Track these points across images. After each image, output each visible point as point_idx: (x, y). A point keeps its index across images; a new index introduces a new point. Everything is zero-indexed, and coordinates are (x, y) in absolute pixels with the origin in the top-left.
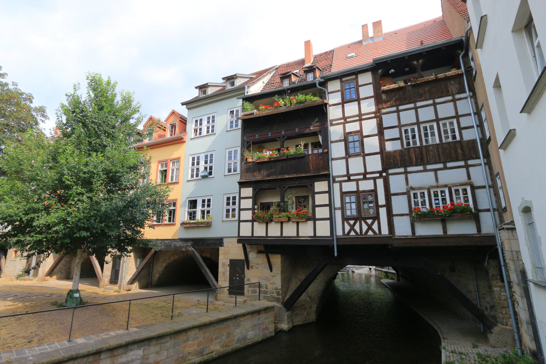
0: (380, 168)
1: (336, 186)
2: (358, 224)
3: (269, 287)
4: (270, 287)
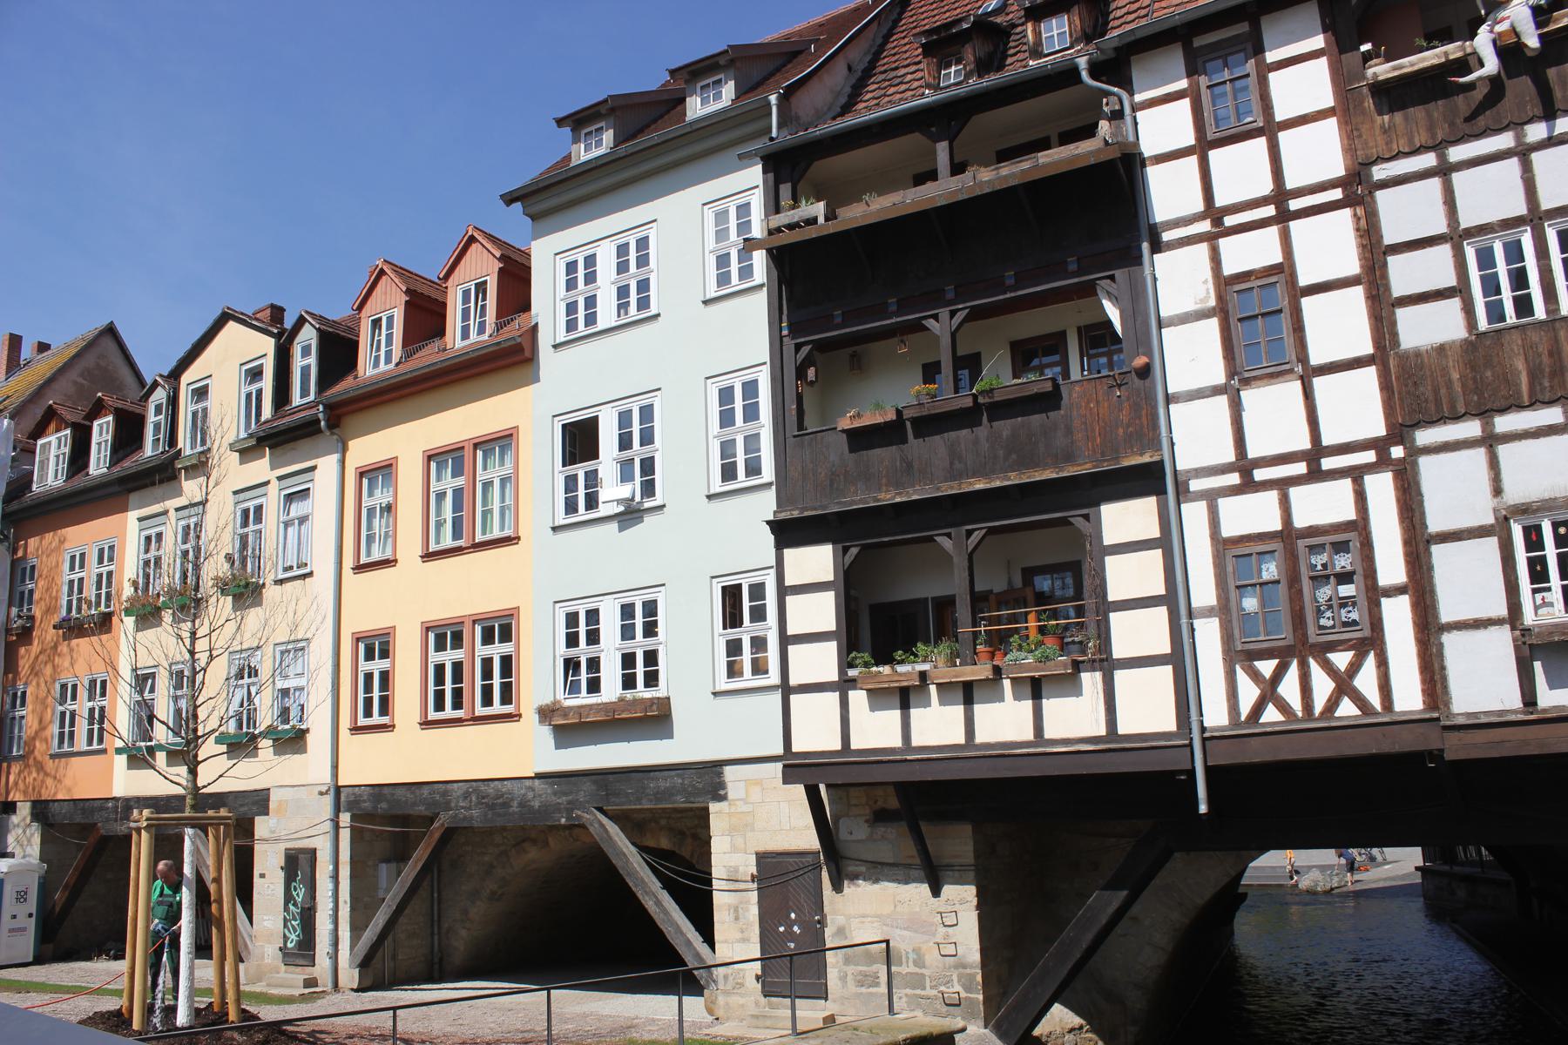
0: (1380, 430)
1: (1194, 516)
2: (1293, 672)
4: (932, 957)
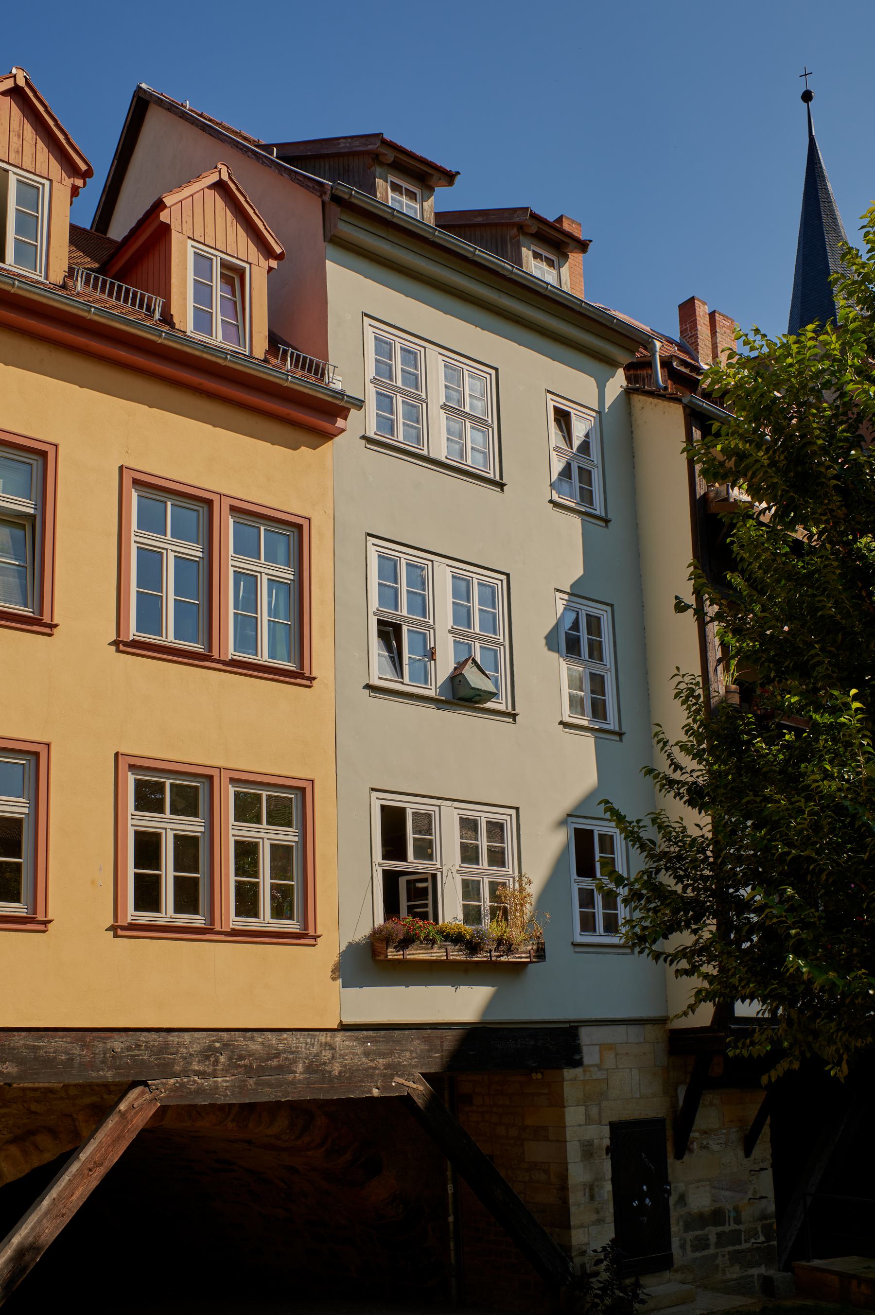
3: (744, 1216)
